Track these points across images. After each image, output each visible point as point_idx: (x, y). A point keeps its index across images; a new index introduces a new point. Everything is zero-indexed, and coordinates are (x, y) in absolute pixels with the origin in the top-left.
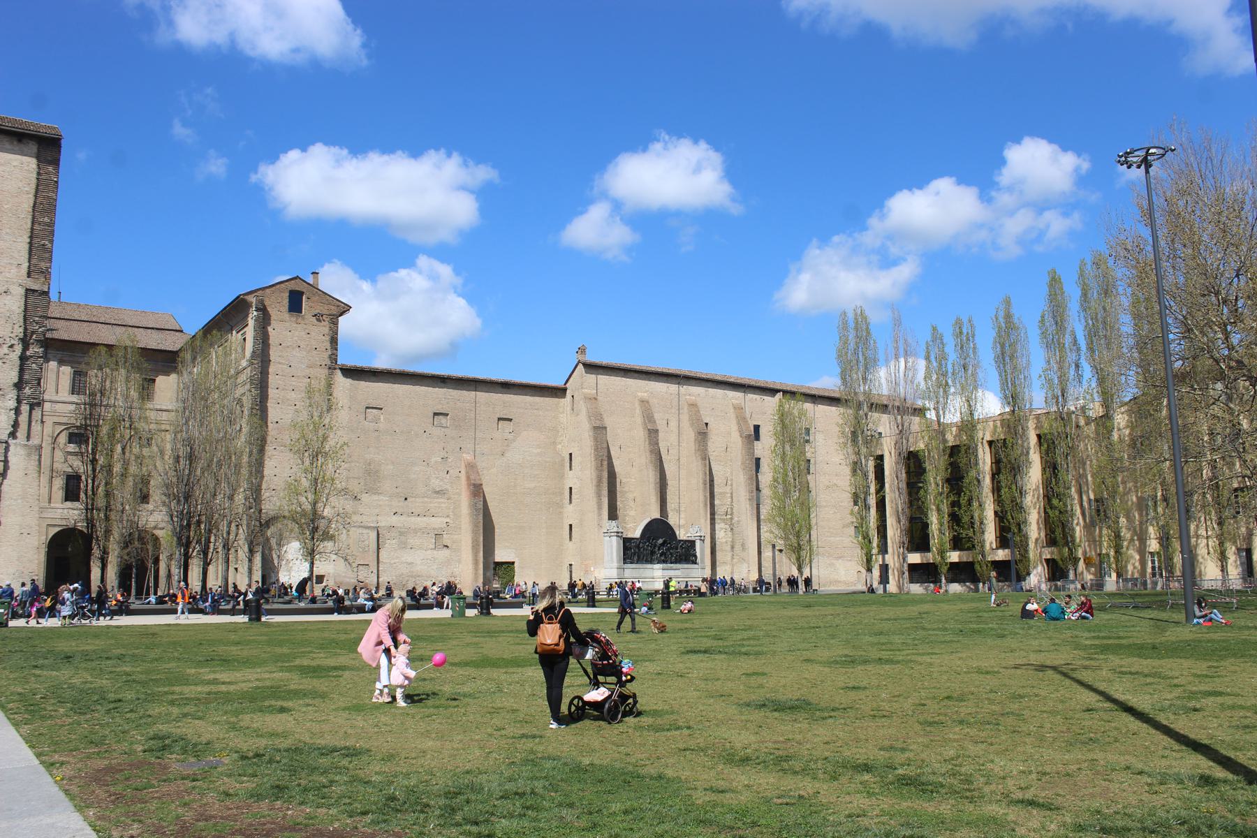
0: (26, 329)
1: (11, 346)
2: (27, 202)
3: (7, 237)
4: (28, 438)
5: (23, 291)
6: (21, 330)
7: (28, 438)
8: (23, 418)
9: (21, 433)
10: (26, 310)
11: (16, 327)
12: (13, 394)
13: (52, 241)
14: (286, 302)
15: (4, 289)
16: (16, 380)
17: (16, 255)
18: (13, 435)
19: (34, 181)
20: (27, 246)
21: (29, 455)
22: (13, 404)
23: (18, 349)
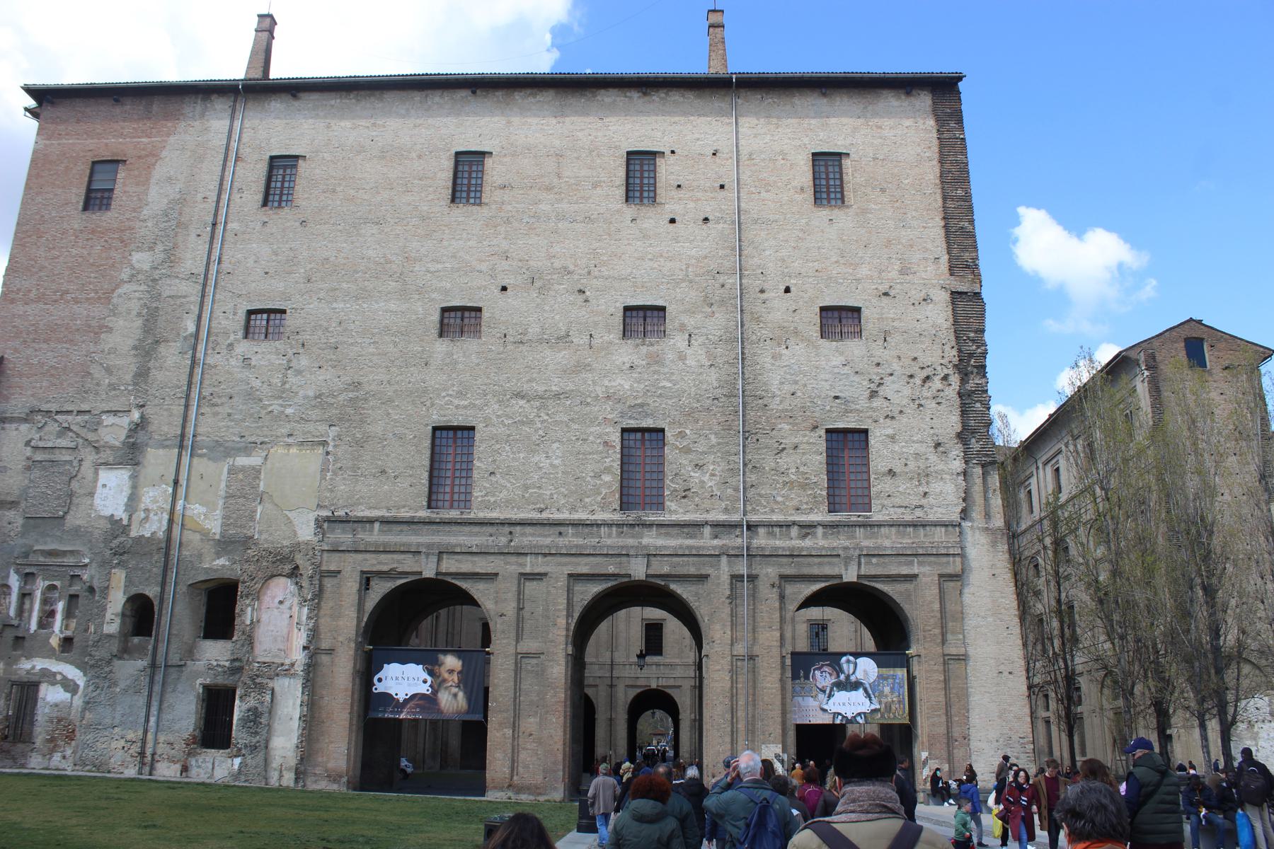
0: (960, 351)
1: (945, 378)
2: (931, 172)
3: (915, 223)
4: (988, 516)
5: (946, 296)
6: (954, 352)
7: (988, 516)
8: (977, 489)
9: (977, 513)
10: (955, 322)
11: (947, 348)
12: (956, 451)
13: (972, 222)
14: (1182, 355)
15: (922, 295)
16: (958, 428)
17: (929, 246)
18: (965, 514)
19: (936, 142)
20: (942, 232)
21: (994, 544)
22: (958, 465)
23: (955, 380)
